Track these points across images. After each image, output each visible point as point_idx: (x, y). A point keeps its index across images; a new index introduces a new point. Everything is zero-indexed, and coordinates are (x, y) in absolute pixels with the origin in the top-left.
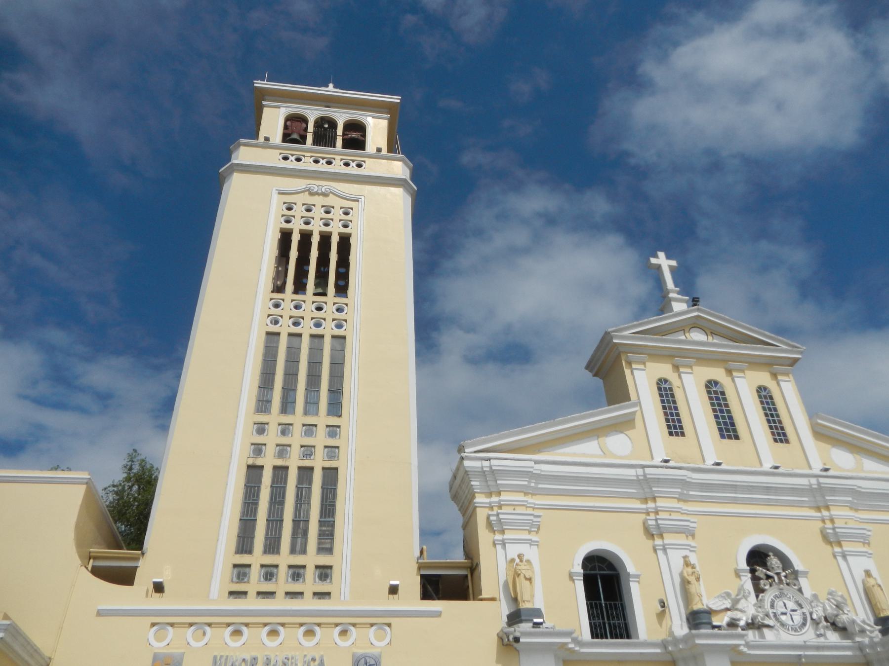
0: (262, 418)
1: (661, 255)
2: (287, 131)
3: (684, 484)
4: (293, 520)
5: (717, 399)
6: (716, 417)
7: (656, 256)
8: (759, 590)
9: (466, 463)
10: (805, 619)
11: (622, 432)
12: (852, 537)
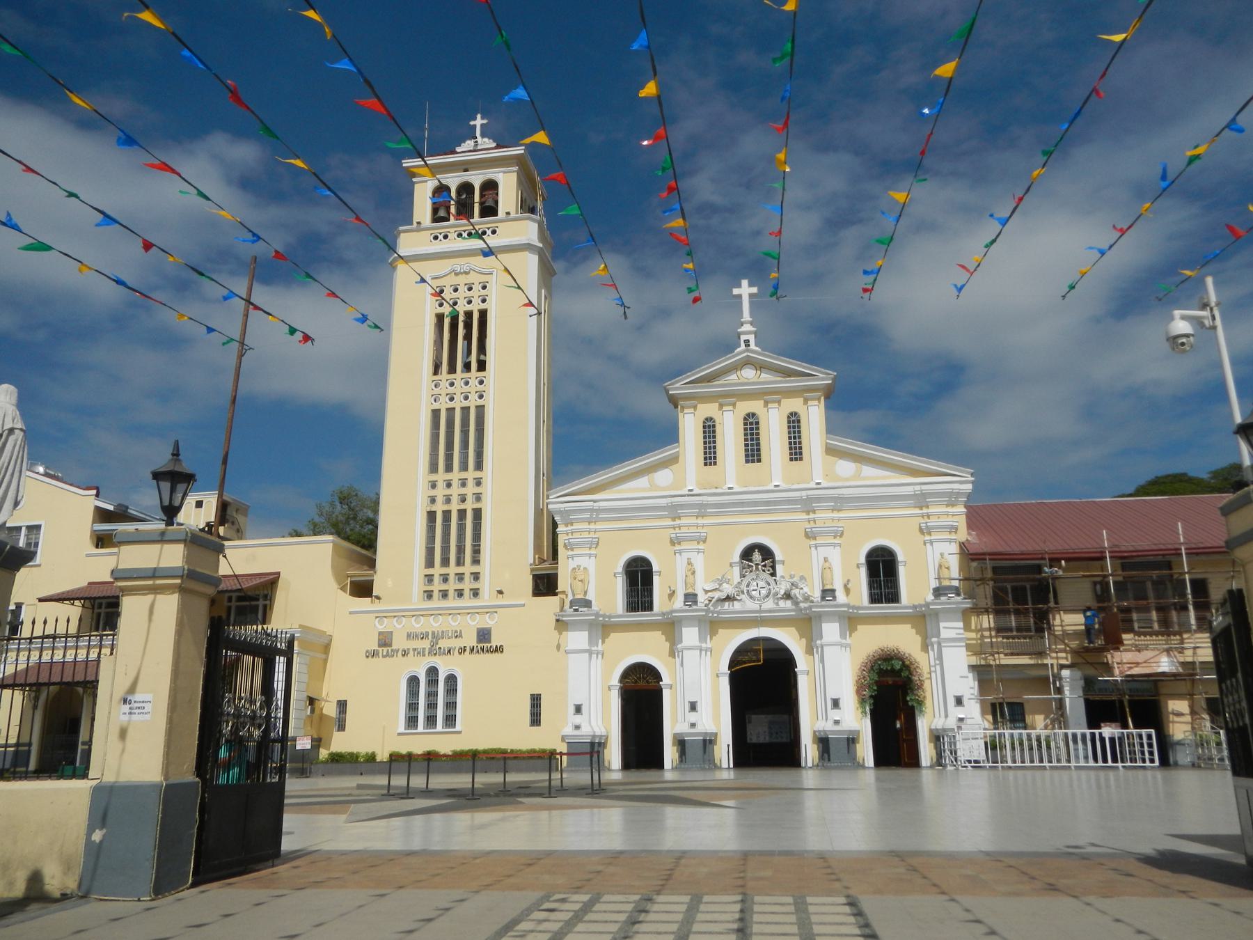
0: (434, 477)
1: (745, 283)
2: (437, 206)
3: (702, 506)
4: (457, 546)
5: (752, 429)
6: (746, 445)
7: (739, 286)
9: (550, 506)
10: (769, 593)
11: (666, 468)
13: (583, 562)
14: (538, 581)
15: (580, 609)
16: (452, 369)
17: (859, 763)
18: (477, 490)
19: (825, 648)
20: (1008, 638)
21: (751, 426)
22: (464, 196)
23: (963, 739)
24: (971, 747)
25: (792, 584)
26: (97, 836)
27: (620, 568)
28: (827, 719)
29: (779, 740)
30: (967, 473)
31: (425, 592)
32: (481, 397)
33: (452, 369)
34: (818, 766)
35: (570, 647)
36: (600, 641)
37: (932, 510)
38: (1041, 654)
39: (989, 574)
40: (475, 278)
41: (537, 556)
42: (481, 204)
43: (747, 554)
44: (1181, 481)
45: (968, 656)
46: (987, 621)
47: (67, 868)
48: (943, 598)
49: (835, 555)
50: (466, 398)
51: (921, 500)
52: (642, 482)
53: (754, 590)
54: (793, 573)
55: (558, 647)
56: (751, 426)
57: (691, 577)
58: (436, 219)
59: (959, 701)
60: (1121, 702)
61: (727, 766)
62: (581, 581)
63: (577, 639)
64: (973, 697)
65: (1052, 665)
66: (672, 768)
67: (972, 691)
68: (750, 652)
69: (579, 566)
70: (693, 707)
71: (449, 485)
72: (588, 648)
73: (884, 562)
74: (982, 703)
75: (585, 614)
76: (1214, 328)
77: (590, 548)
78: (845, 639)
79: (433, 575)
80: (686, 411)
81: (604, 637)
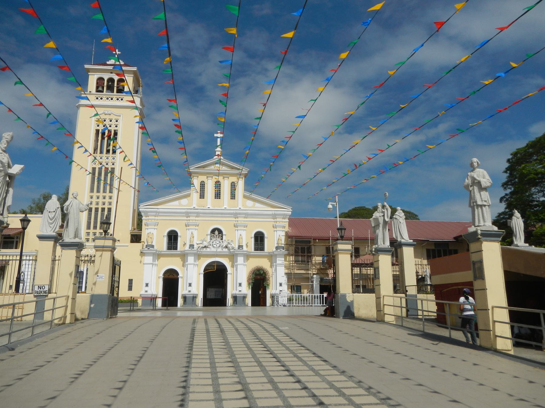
0: (92, 194)
2: (98, 85)
3: (198, 213)
10: (220, 246)
12: (241, 226)
13: (152, 231)
14: (133, 237)
15: (150, 248)
16: (101, 152)
17: (246, 305)
18: (110, 201)
19: (238, 265)
20: (298, 264)
21: (218, 185)
22: (110, 83)
23: (281, 297)
24: (283, 300)
25: (228, 243)
26: (92, 306)
27: (166, 234)
28: (236, 290)
29: (218, 297)
30: (289, 208)
31: (86, 239)
32: (113, 164)
33: (101, 152)
34: (232, 306)
35: (145, 262)
36: (157, 260)
37: (277, 220)
38: (308, 270)
39: (294, 243)
40: (113, 118)
41: (133, 227)
42: (117, 87)
43: (213, 231)
44: (363, 209)
45: (285, 269)
46: (292, 258)
47: (82, 312)
48: (279, 250)
49: (244, 234)
50: (107, 164)
51: (274, 216)
52: (176, 203)
53: (215, 244)
54: (229, 239)
55: (141, 262)
56: (218, 185)
57: (192, 238)
58: (98, 91)
59: (281, 285)
60: (330, 286)
61: (200, 306)
62: (151, 238)
63: (148, 259)
64: (285, 283)
65: (311, 273)
66: (181, 306)
67: (285, 281)
68: (211, 266)
69: (150, 233)
70: (190, 285)
72: (152, 263)
73: (260, 237)
74: (288, 285)
75: (152, 250)
76: (337, 207)
77: (155, 226)
78: (245, 262)
79: (90, 232)
80: (194, 178)
81: (158, 259)
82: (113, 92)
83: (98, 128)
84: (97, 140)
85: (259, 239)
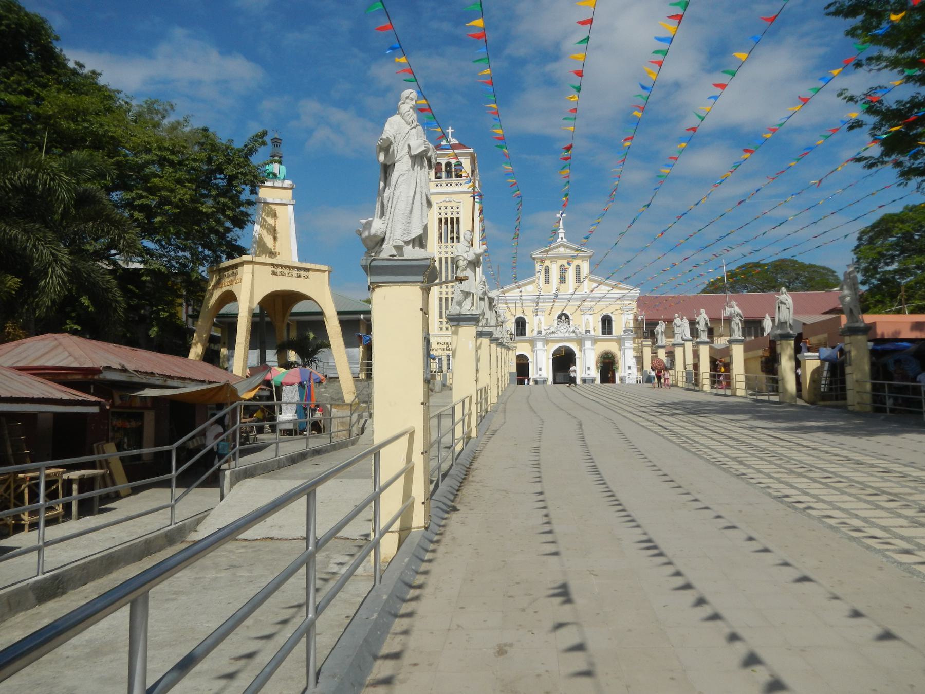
8: (558, 324)
21: (563, 270)
40: (453, 204)
43: (559, 317)
49: (591, 318)
50: (452, 253)
56: (563, 270)
58: (437, 178)
59: (629, 368)
70: (540, 369)
71: (447, 287)
73: (608, 320)
82: (451, 177)
83: (440, 217)
84: (440, 228)
85: (607, 323)
